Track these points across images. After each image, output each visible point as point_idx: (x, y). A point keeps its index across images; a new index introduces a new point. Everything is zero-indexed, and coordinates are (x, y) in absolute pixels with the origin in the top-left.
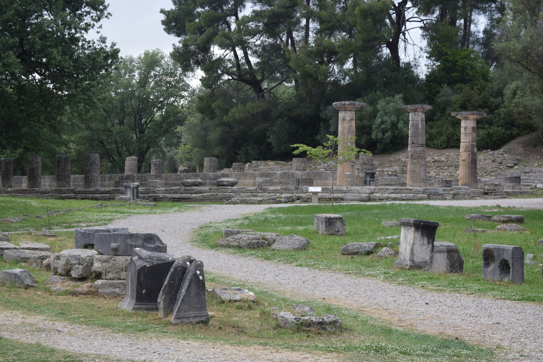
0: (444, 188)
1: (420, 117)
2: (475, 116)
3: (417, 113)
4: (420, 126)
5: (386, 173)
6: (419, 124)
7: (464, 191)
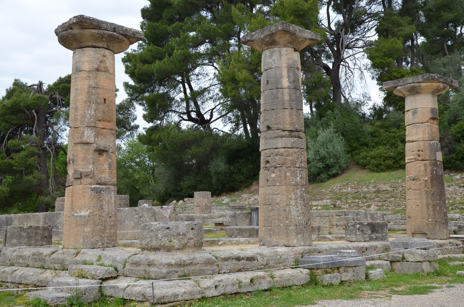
0: (366, 244)
1: (283, 57)
2: (435, 84)
3: (275, 49)
4: (285, 83)
5: (315, 208)
6: (281, 77)
7: (420, 251)
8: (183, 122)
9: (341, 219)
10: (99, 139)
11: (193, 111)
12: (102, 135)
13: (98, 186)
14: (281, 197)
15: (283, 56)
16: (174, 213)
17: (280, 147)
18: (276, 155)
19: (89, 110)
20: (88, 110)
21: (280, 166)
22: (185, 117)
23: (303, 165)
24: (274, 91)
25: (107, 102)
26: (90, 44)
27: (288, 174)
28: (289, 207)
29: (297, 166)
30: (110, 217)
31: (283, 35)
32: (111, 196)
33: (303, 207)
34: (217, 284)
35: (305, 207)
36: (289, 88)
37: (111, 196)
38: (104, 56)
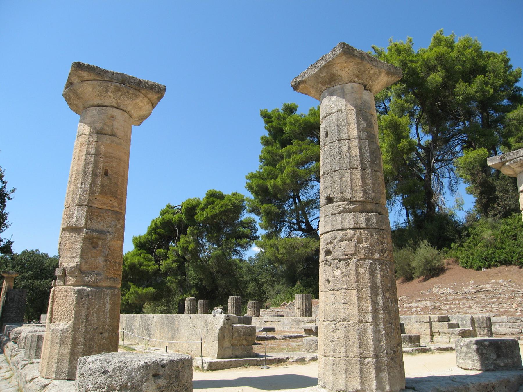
5: (415, 309)
8: (294, 232)
9: (443, 326)
10: (93, 222)
11: (303, 222)
12: (97, 216)
13: (84, 288)
14: (350, 308)
15: (348, 95)
16: (227, 323)
17: (347, 227)
18: (341, 241)
19: (83, 183)
20: (82, 184)
21: (347, 257)
22: (296, 227)
23: (386, 255)
24: (336, 145)
25: (110, 172)
26: (95, 103)
27: (361, 270)
28: (365, 326)
30: (101, 333)
31: (345, 65)
32: (104, 302)
33: (388, 325)
35: (391, 324)
37: (104, 302)
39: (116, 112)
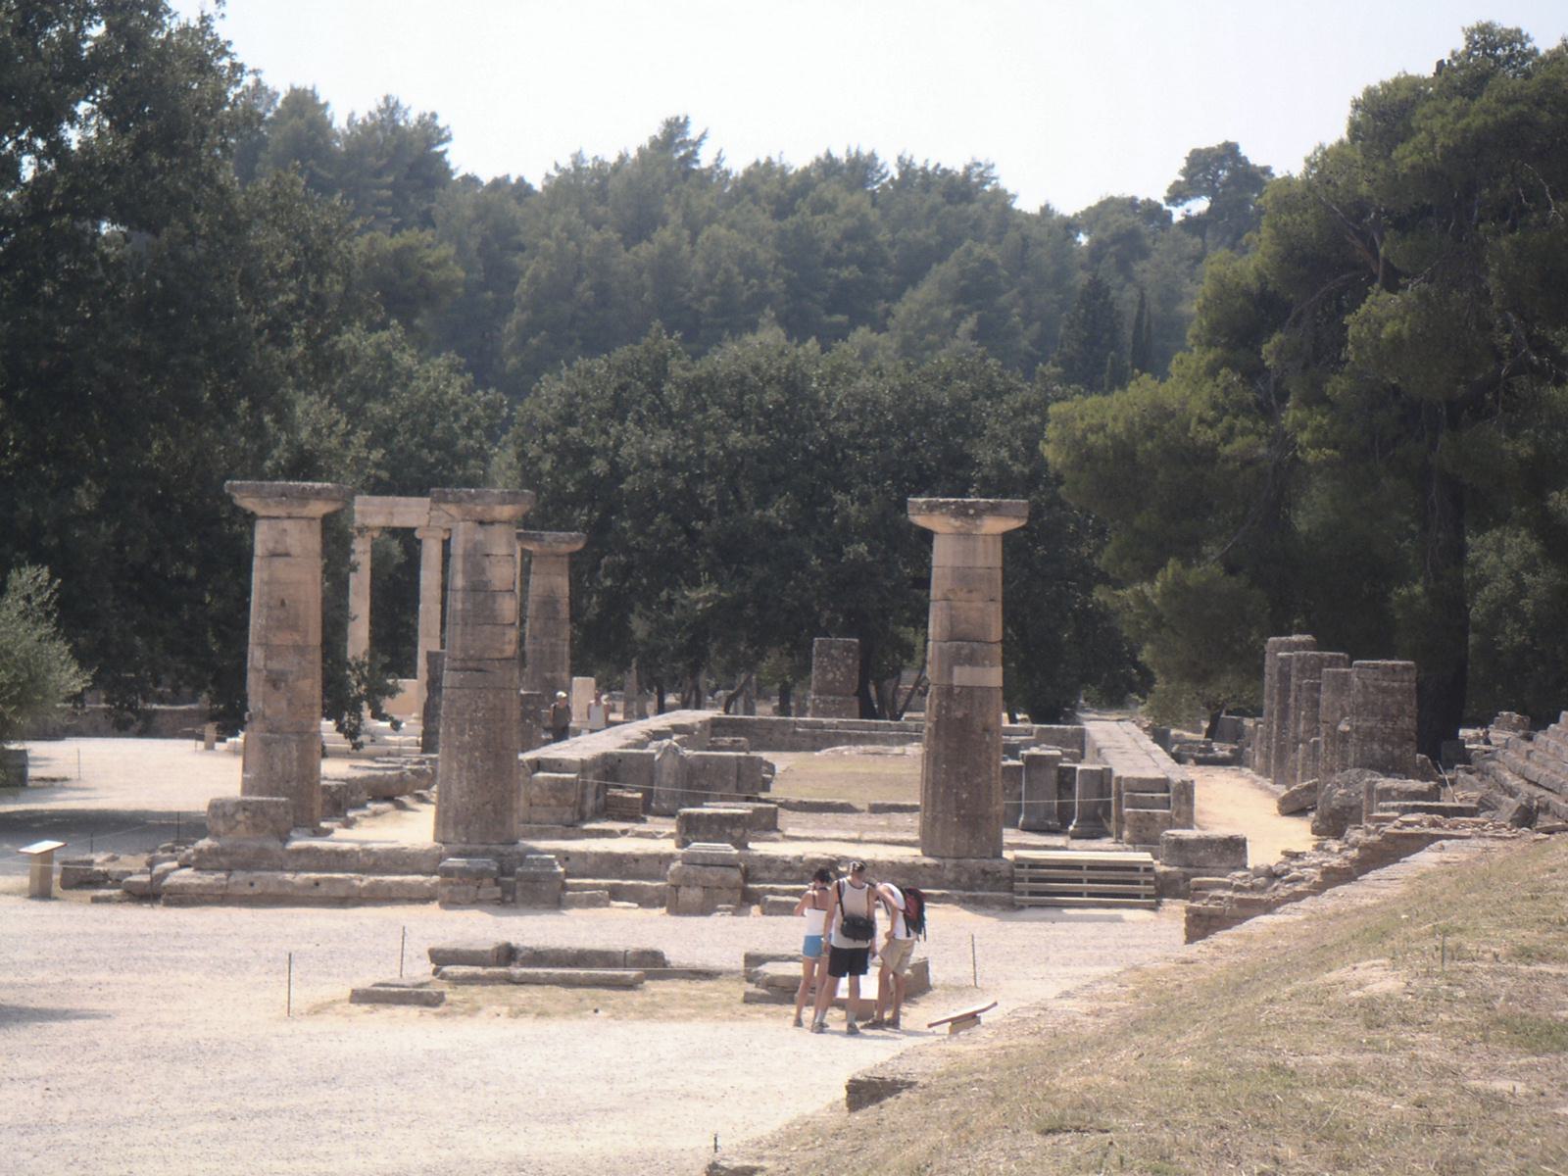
13: (268, 735)
25: (287, 602)
29: (467, 716)
34: (252, 880)
36: (464, 589)
38: (285, 530)
39: (287, 524)
